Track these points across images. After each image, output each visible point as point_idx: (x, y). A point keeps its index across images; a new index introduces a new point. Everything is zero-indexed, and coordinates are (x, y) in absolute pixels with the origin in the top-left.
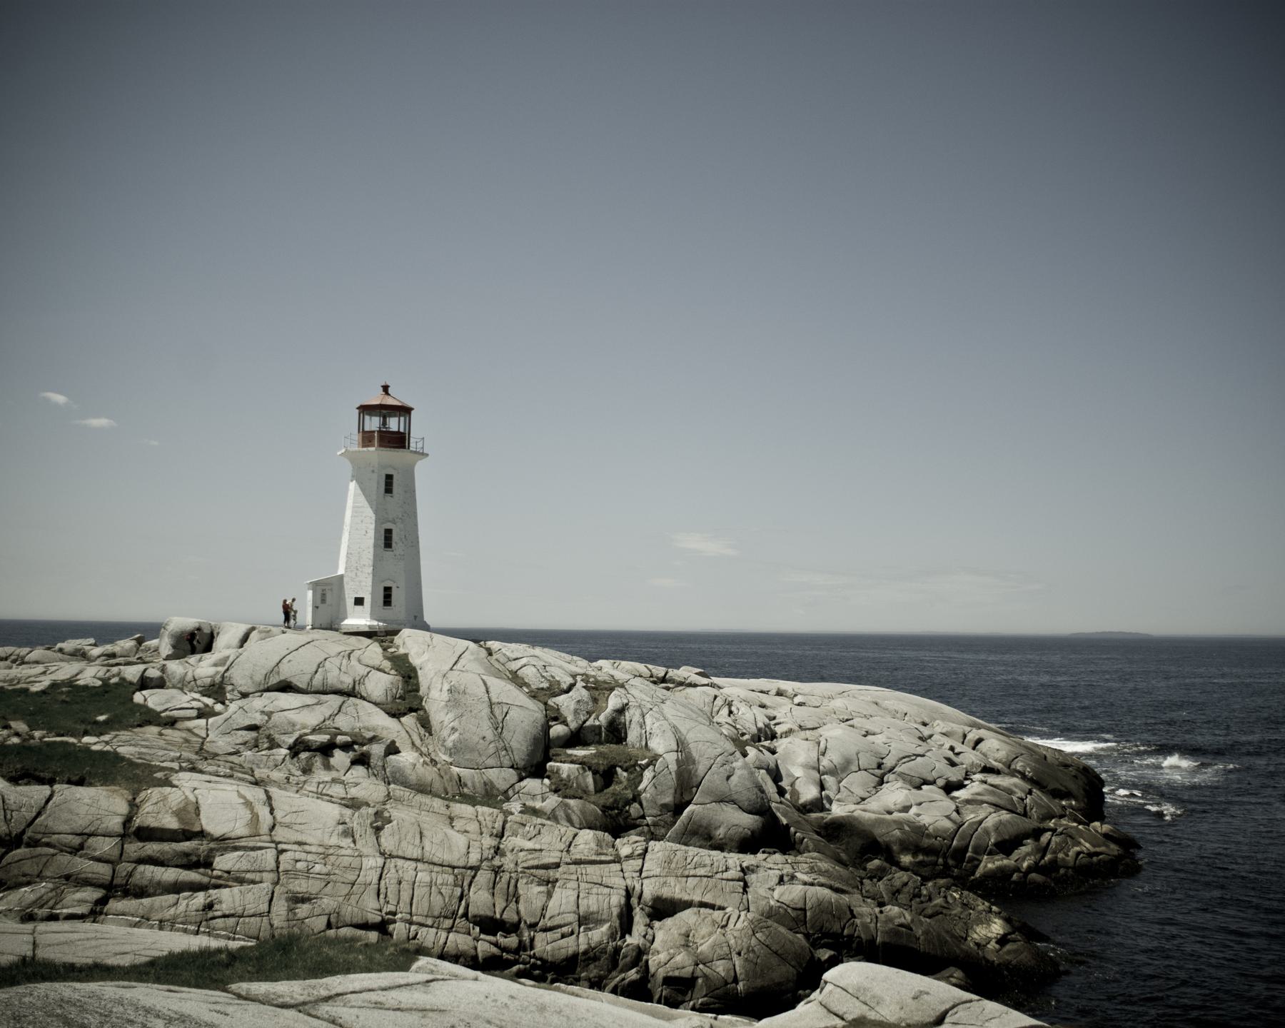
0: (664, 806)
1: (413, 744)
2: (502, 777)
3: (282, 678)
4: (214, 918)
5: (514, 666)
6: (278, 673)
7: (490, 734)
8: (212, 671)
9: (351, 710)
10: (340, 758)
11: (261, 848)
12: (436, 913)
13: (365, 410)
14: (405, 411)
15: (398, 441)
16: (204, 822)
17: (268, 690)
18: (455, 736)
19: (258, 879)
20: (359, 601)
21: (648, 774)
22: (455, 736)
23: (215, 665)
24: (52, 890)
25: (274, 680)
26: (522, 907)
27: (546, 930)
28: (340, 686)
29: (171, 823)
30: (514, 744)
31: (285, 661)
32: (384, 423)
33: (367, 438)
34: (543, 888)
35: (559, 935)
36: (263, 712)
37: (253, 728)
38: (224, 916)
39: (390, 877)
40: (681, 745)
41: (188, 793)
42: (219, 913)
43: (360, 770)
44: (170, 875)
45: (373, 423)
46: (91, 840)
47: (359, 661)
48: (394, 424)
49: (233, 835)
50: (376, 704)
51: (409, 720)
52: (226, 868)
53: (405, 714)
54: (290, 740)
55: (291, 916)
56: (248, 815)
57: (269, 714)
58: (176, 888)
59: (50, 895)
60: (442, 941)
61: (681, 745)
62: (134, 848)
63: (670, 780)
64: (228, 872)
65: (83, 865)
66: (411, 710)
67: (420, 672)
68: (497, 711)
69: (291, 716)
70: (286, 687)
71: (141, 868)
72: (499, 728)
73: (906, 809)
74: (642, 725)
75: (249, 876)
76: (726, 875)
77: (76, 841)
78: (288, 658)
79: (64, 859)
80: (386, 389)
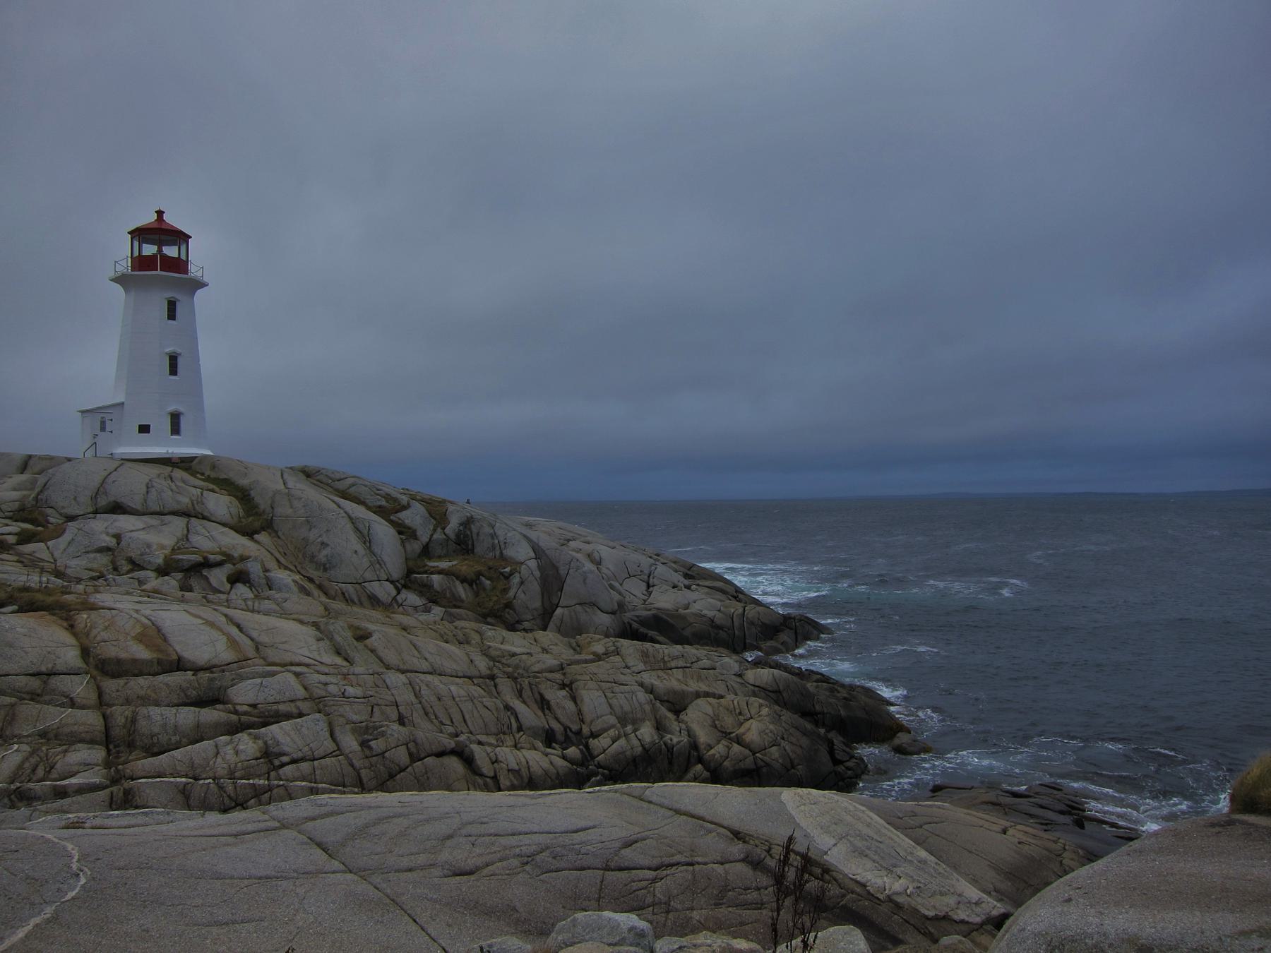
0: (536, 609)
1: (278, 561)
2: (384, 591)
3: (112, 499)
4: (283, 765)
5: (341, 485)
6: (106, 493)
7: (361, 551)
8: (16, 495)
9: (200, 528)
10: (218, 577)
11: (273, 674)
12: (494, 730)
13: (140, 234)
14: (180, 238)
15: (179, 265)
16: (178, 648)
17: (96, 512)
18: (324, 552)
19: (295, 711)
20: (144, 429)
21: (516, 580)
23: (15, 490)
24: (32, 754)
25: (103, 502)
26: (559, 713)
27: (594, 735)
28: (176, 507)
29: (142, 653)
30: (386, 558)
31: (109, 480)
32: (160, 250)
33: (142, 263)
34: (563, 693)
35: (609, 741)
36: (108, 534)
38: (294, 761)
39: (425, 691)
40: (538, 552)
41: (135, 615)
42: (285, 759)
43: (241, 589)
44: (187, 716)
45: (150, 249)
46: (55, 682)
47: (184, 482)
48: (171, 251)
49: (215, 661)
50: (224, 525)
51: (263, 537)
52: (251, 698)
53: (257, 532)
54: (160, 561)
55: (367, 752)
56: (224, 639)
57: (118, 537)
58: (198, 735)
59: (34, 760)
60: (523, 760)
61: (538, 552)
62: (110, 685)
63: (535, 587)
64: (254, 706)
65: (55, 716)
66: (263, 529)
67: (253, 493)
68: (361, 526)
69: (142, 536)
70: (117, 508)
71: (143, 711)
72: (366, 539)
73: (687, 607)
74: (494, 536)
75: (282, 708)
76: (701, 664)
77: (35, 683)
78: (112, 477)
79: (28, 709)
80: (160, 213)
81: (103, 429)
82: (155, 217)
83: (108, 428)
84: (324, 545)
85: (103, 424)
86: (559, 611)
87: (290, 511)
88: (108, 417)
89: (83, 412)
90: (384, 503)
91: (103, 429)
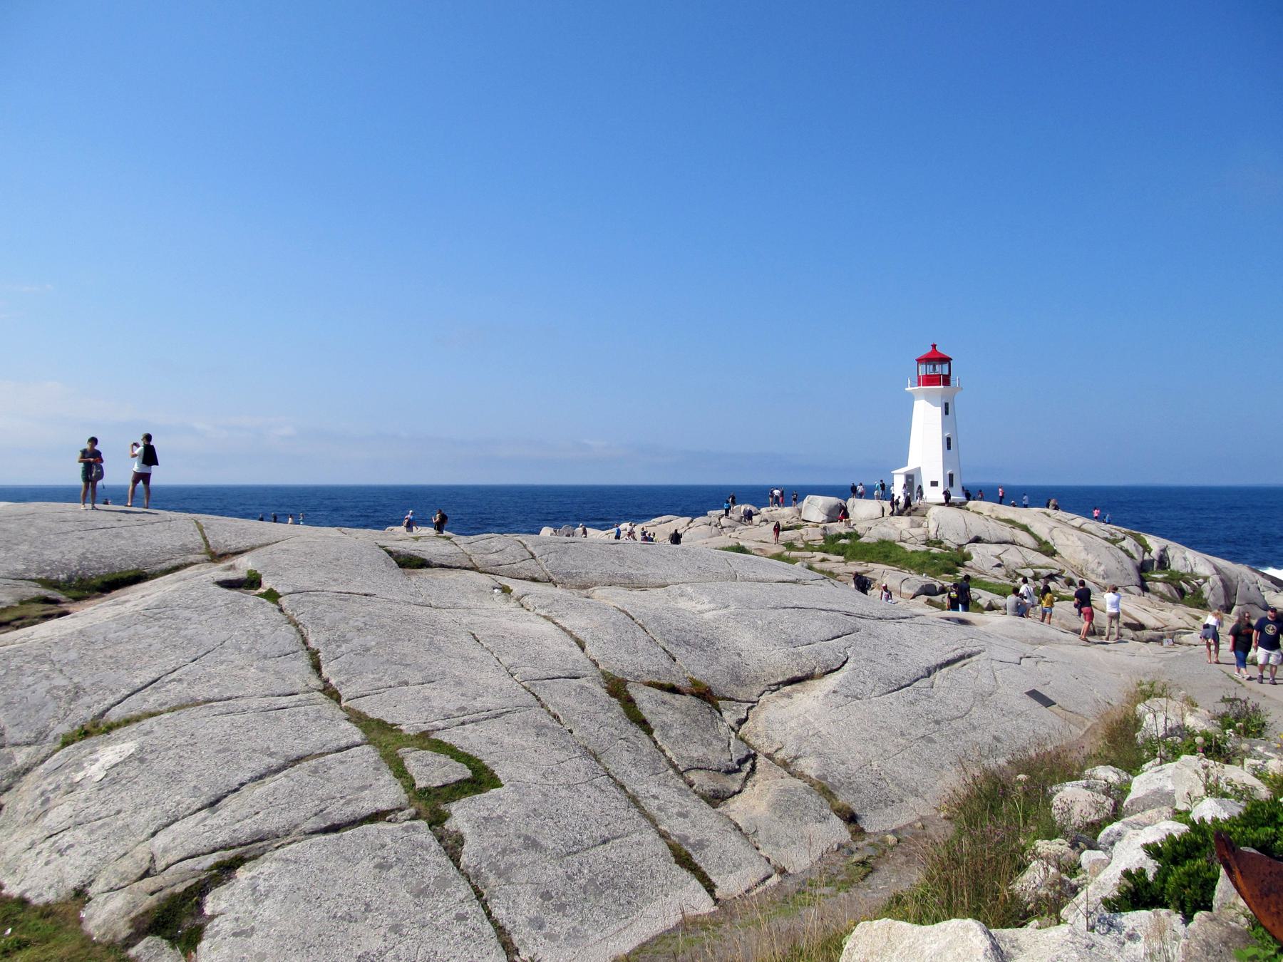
14: (946, 360)
18: (1102, 568)
20: (934, 484)
22: (1102, 568)
37: (999, 566)
57: (998, 557)
63: (1221, 591)
70: (977, 540)
74: (1185, 559)
80: (934, 346)
82: (930, 349)
86: (1235, 609)
90: (1108, 535)
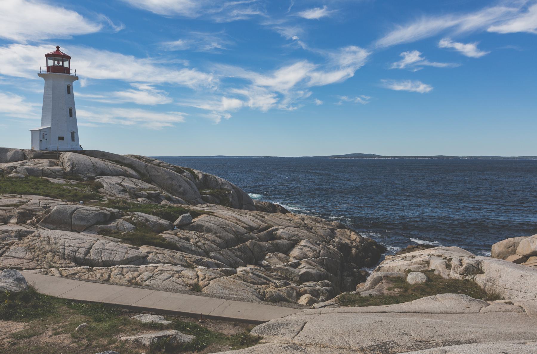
14: (68, 58)
18: (182, 189)
20: (61, 138)
57: (120, 184)
81: (43, 138)
83: (45, 138)
84: (180, 186)
85: (43, 135)
87: (159, 174)
88: (45, 133)
89: (31, 131)
91: (43, 138)
